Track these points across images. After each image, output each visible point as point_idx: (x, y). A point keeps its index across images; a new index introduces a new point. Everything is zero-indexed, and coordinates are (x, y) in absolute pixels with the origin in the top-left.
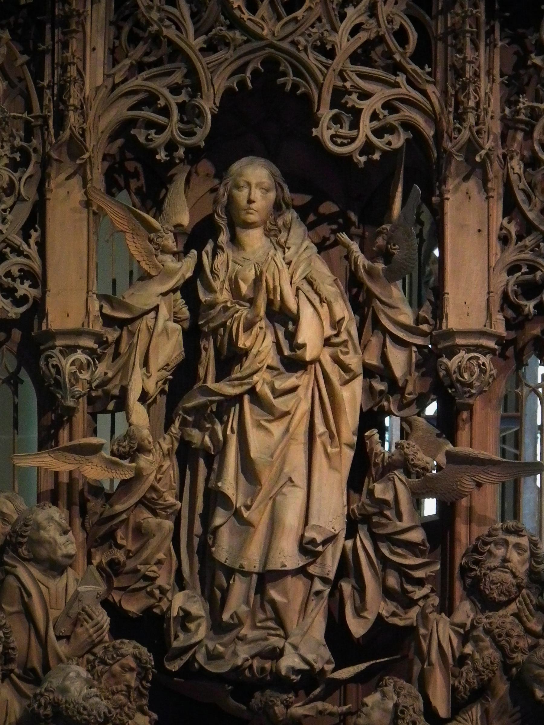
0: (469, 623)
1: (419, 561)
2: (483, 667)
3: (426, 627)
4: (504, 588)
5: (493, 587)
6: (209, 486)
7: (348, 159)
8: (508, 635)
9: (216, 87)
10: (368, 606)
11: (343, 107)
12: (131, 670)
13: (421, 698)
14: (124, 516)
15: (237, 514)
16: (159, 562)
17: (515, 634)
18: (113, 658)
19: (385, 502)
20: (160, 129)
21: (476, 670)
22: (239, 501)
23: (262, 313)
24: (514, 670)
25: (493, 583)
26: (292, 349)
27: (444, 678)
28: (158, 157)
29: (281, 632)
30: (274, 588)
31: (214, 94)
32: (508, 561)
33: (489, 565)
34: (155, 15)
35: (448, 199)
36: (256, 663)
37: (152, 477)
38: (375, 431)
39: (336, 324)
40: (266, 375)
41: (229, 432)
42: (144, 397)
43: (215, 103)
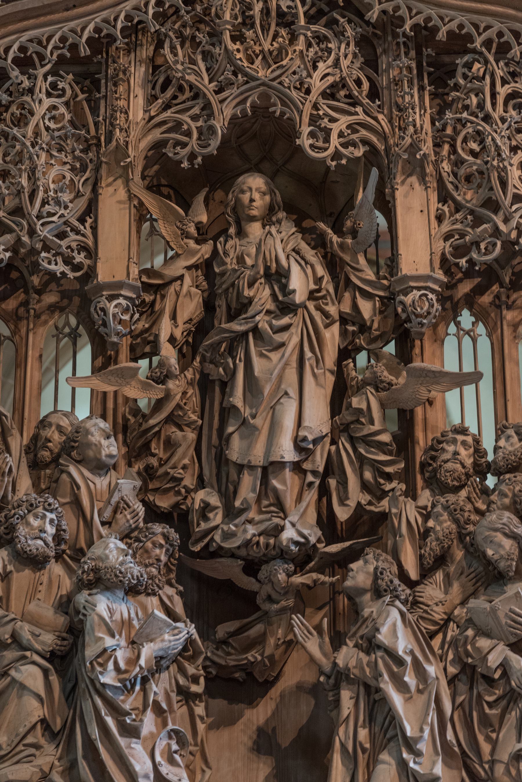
0: (430, 505)
1: (388, 458)
2: (444, 536)
3: (396, 507)
4: (456, 475)
5: (448, 474)
6: (224, 406)
7: (323, 161)
8: (461, 510)
9: (225, 114)
10: (350, 495)
11: (319, 127)
12: (161, 546)
13: (395, 564)
14: (157, 429)
15: (244, 422)
16: (184, 467)
17: (467, 509)
18: (146, 536)
19: (359, 411)
20: (184, 145)
21: (437, 539)
22: (247, 412)
23: (262, 272)
24: (468, 538)
25: (447, 471)
26: (285, 295)
27: (413, 548)
28: (182, 166)
29: (282, 515)
30: (275, 478)
31: (224, 119)
32: (458, 454)
33: (443, 458)
34: (180, 67)
35: (398, 189)
36: (262, 540)
37: (178, 397)
38: (351, 360)
39: (318, 280)
40: (267, 318)
41: (237, 361)
42: (172, 340)
43: (224, 125)
